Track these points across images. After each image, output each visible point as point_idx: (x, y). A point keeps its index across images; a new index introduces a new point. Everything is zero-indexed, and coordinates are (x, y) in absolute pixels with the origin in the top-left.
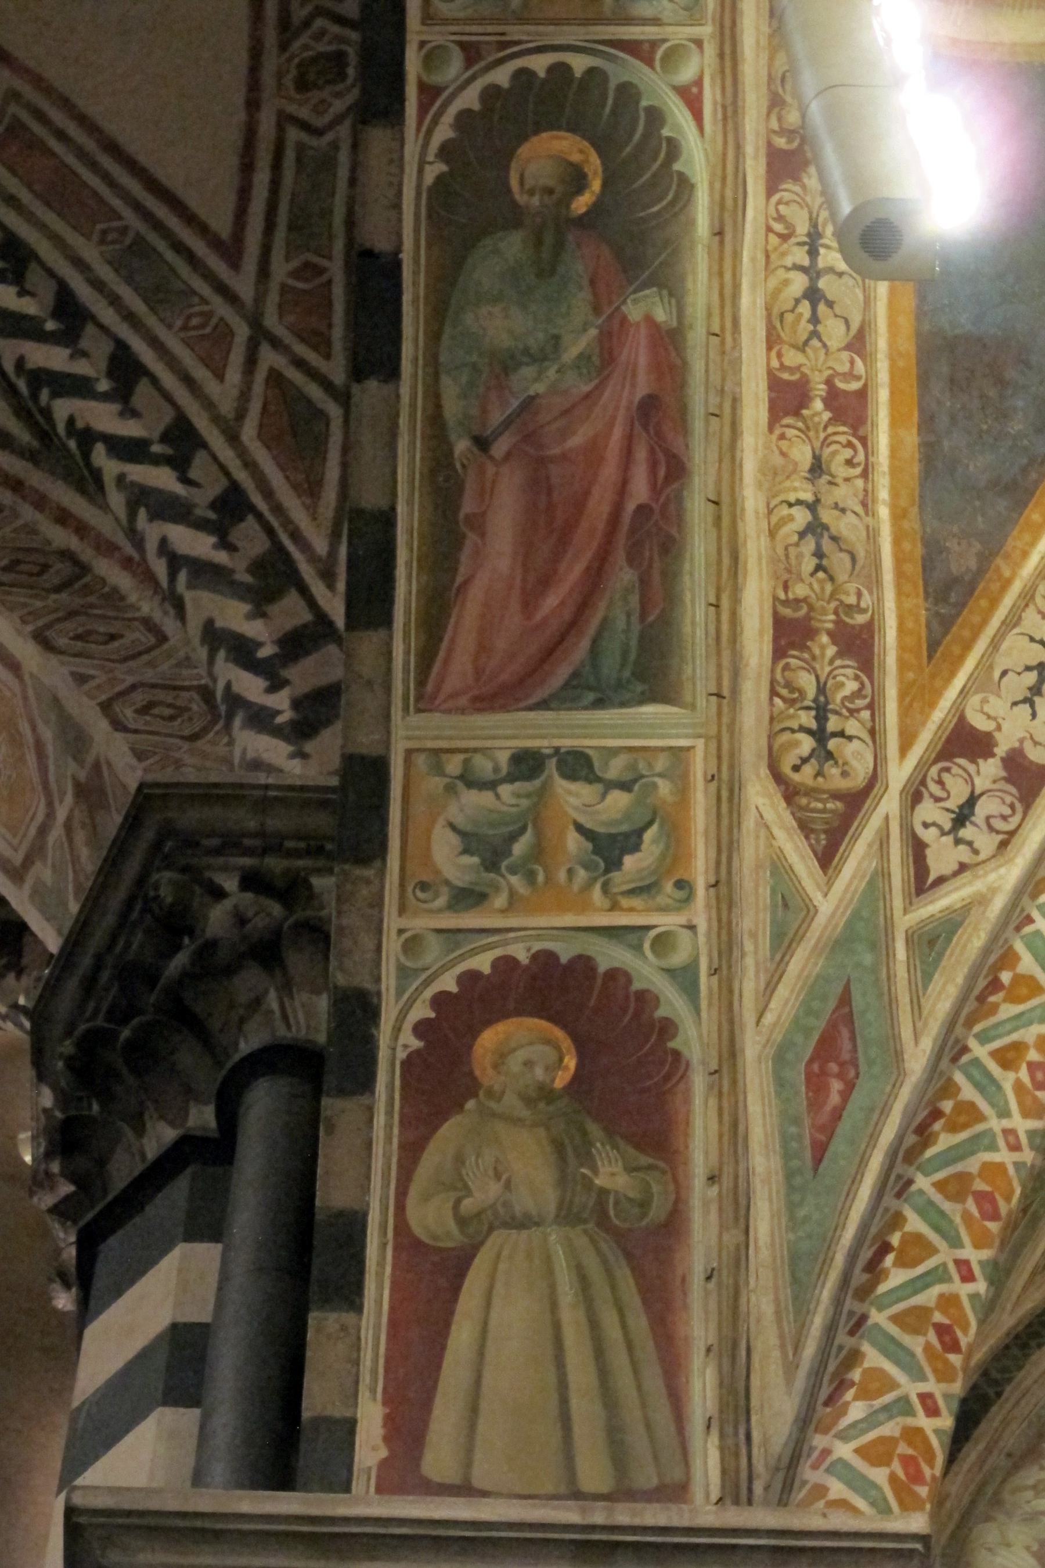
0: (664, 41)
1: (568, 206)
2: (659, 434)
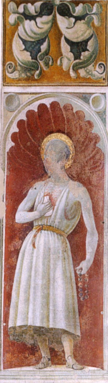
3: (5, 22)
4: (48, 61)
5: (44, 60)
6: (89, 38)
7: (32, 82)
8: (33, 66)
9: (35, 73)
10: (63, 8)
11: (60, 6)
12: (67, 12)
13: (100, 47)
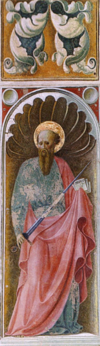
0: (86, 87)
1: (54, 149)
2: (85, 231)
3: (3, 20)
4: (42, 57)
5: (39, 56)
6: (81, 34)
7: (28, 77)
8: (29, 62)
9: (31, 68)
10: (56, 6)
11: (54, 4)
12: (60, 10)
13: (91, 43)
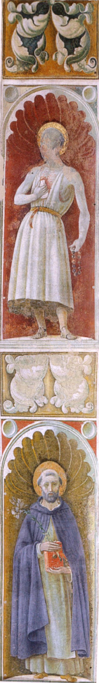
4: (44, 56)
5: (40, 55)
6: (82, 35)
7: (30, 75)
8: (30, 61)
9: (32, 67)
10: (57, 8)
11: (55, 6)
12: (61, 11)
13: (92, 43)
